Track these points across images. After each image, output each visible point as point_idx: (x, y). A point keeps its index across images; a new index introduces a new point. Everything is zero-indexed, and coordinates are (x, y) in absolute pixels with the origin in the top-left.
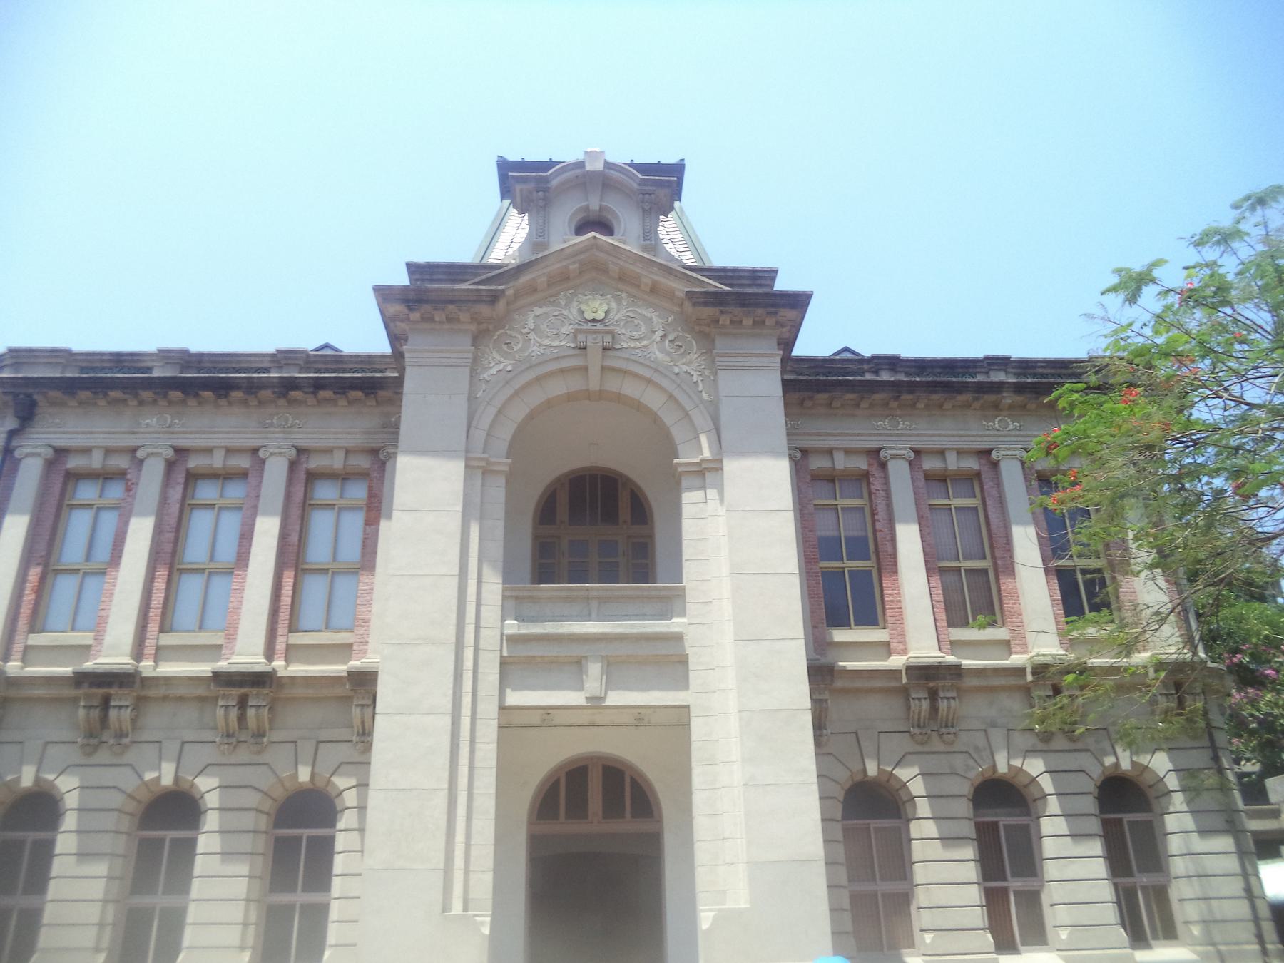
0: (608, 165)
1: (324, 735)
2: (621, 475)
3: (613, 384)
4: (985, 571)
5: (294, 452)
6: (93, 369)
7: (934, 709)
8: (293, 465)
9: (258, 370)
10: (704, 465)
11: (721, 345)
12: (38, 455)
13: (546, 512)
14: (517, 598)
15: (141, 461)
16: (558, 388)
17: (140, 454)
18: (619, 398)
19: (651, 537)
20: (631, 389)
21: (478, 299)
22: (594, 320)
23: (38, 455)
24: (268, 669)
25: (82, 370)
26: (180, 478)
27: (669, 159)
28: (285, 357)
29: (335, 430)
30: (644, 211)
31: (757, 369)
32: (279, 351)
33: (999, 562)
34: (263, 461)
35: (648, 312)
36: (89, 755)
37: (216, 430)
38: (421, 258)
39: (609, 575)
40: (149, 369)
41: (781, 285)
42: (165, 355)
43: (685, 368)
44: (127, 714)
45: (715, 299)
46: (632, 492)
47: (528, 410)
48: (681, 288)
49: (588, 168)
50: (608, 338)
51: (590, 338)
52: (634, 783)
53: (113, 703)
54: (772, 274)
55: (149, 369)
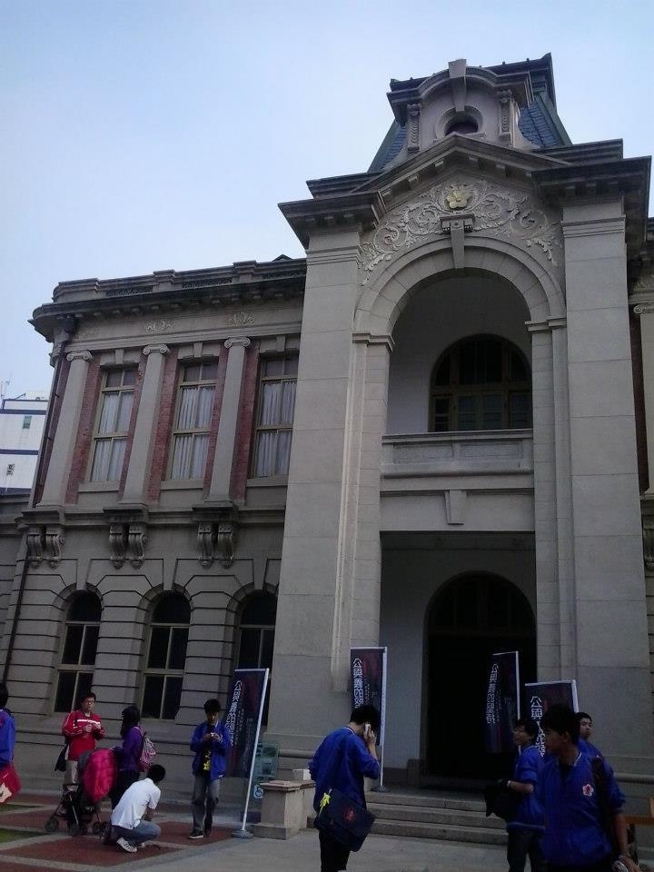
0: (471, 70)
2: (502, 339)
3: (476, 262)
6: (115, 291)
9: (223, 280)
10: (551, 324)
11: (569, 216)
13: (440, 377)
14: (394, 444)
16: (429, 269)
17: (146, 351)
18: (482, 273)
20: (489, 264)
21: (356, 201)
22: (458, 209)
24: (230, 505)
25: (108, 292)
26: (173, 366)
27: (536, 55)
28: (241, 268)
29: (263, 322)
30: (503, 105)
31: (602, 233)
32: (236, 264)
35: (504, 195)
37: (195, 329)
38: (318, 177)
39: (492, 422)
40: (151, 287)
41: (629, 153)
42: (160, 277)
43: (536, 240)
44: (139, 538)
45: (564, 173)
47: (405, 292)
48: (529, 169)
49: (452, 76)
50: (469, 222)
51: (453, 223)
53: (47, 533)
54: (617, 145)
55: (151, 287)
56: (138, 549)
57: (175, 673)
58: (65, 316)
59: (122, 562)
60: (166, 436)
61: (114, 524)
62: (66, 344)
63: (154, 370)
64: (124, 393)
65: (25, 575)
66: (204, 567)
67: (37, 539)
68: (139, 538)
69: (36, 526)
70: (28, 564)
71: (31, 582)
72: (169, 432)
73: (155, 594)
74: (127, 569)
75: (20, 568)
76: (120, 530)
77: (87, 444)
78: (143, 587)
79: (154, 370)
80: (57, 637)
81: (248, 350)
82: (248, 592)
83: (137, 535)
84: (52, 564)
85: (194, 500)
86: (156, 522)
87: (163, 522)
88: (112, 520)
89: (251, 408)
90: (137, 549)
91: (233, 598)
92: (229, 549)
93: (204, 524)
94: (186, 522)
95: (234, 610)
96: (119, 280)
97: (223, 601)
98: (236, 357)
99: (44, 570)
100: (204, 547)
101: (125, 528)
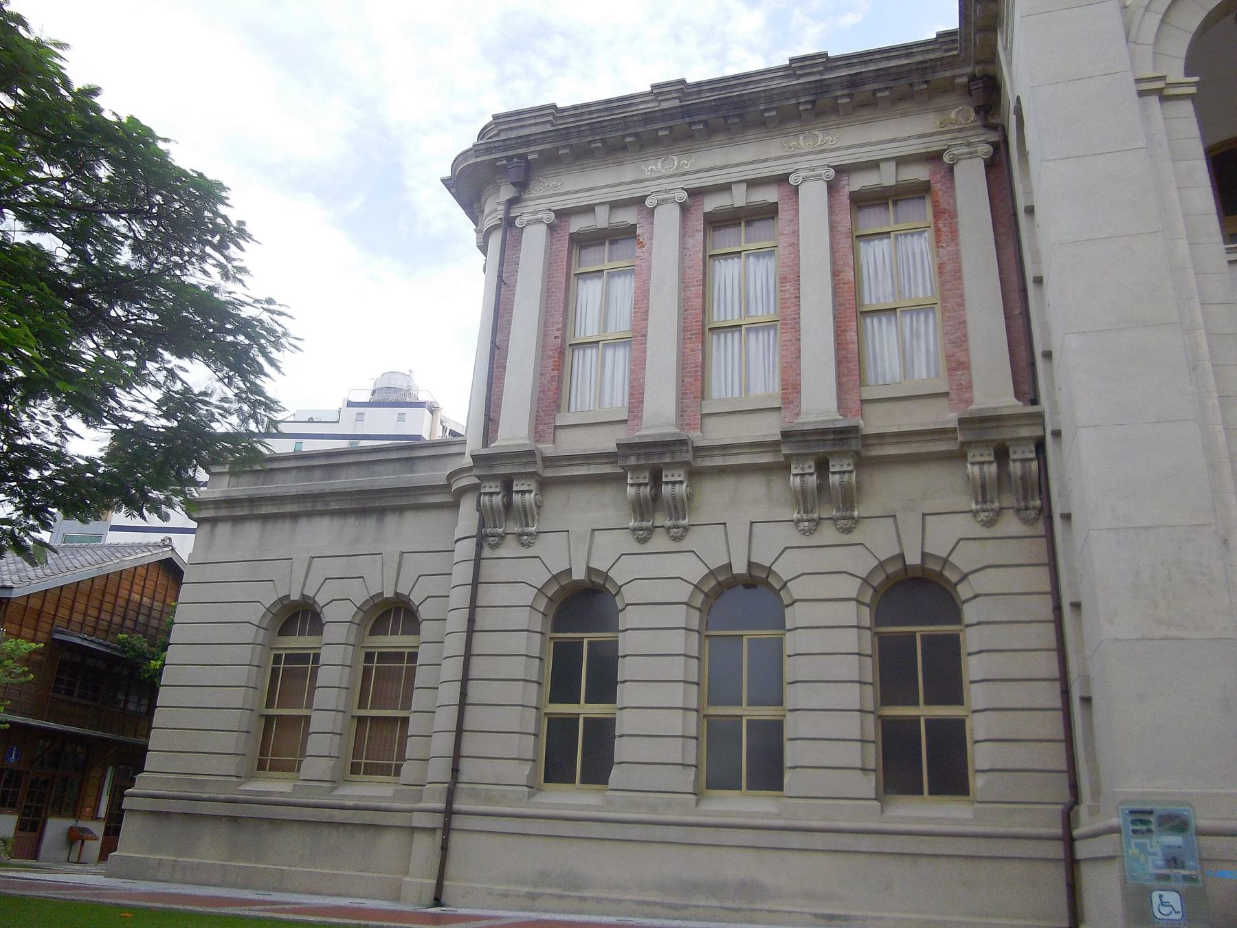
1: (929, 506)
5: (832, 172)
15: (652, 211)
17: (648, 203)
26: (698, 223)
34: (796, 190)
36: (643, 541)
56: (679, 508)
57: (766, 713)
58: (509, 158)
59: (651, 530)
60: (699, 330)
61: (636, 468)
62: (512, 202)
63: (665, 235)
64: (613, 274)
65: (478, 560)
66: (803, 532)
67: (497, 500)
68: (682, 489)
69: (494, 477)
70: (481, 539)
71: (490, 570)
72: (703, 326)
73: (713, 583)
74: (660, 541)
75: (466, 549)
76: (645, 477)
77: (562, 353)
78: (696, 571)
79: (665, 235)
80: (541, 659)
81: (832, 187)
82: (890, 570)
83: (675, 486)
84: (525, 539)
85: (769, 428)
86: (708, 463)
87: (719, 461)
88: (632, 461)
89: (849, 275)
90: (676, 507)
91: (865, 581)
92: (848, 498)
93: (801, 457)
94: (766, 458)
95: (868, 601)
96: (589, 105)
97: (850, 587)
98: (813, 197)
99: (510, 548)
100: (803, 500)
101: (656, 474)
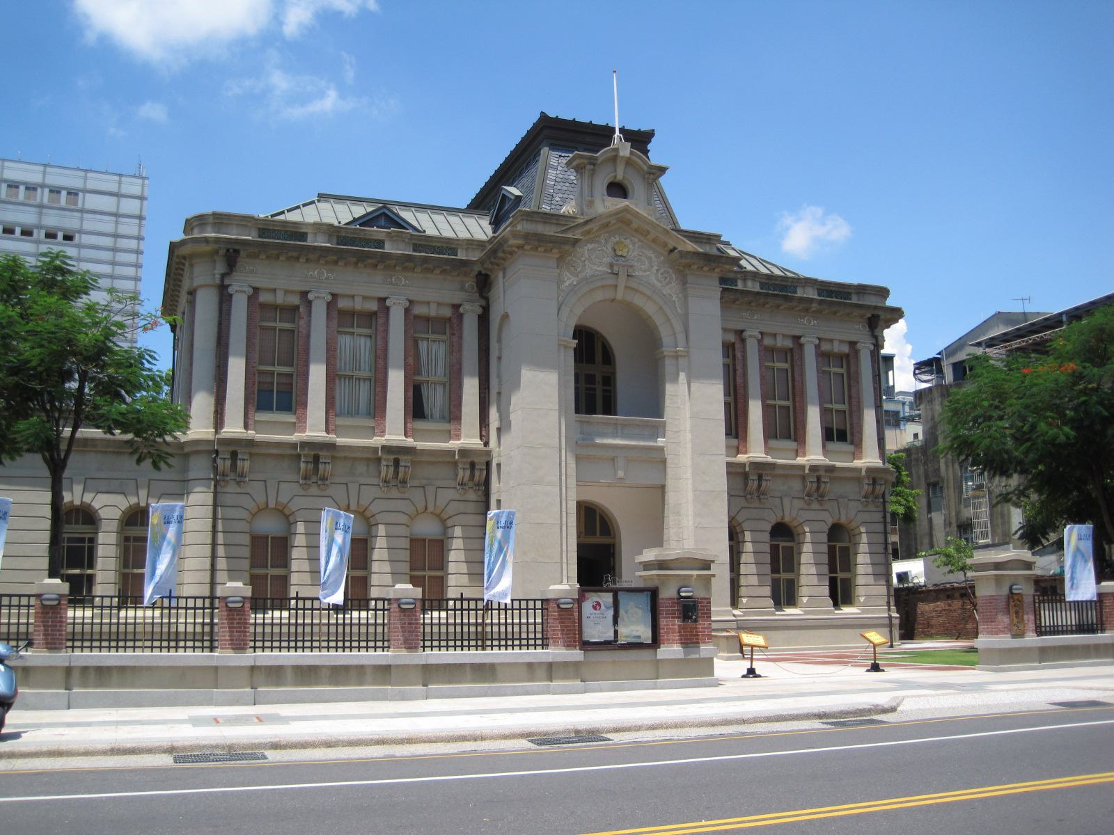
2: (597, 333)
4: (788, 407)
5: (408, 304)
7: (760, 486)
8: (407, 311)
12: (244, 292)
19: (614, 373)
23: (244, 292)
33: (797, 404)
35: (650, 253)
46: (603, 343)
52: (602, 518)
99: (232, 488)
